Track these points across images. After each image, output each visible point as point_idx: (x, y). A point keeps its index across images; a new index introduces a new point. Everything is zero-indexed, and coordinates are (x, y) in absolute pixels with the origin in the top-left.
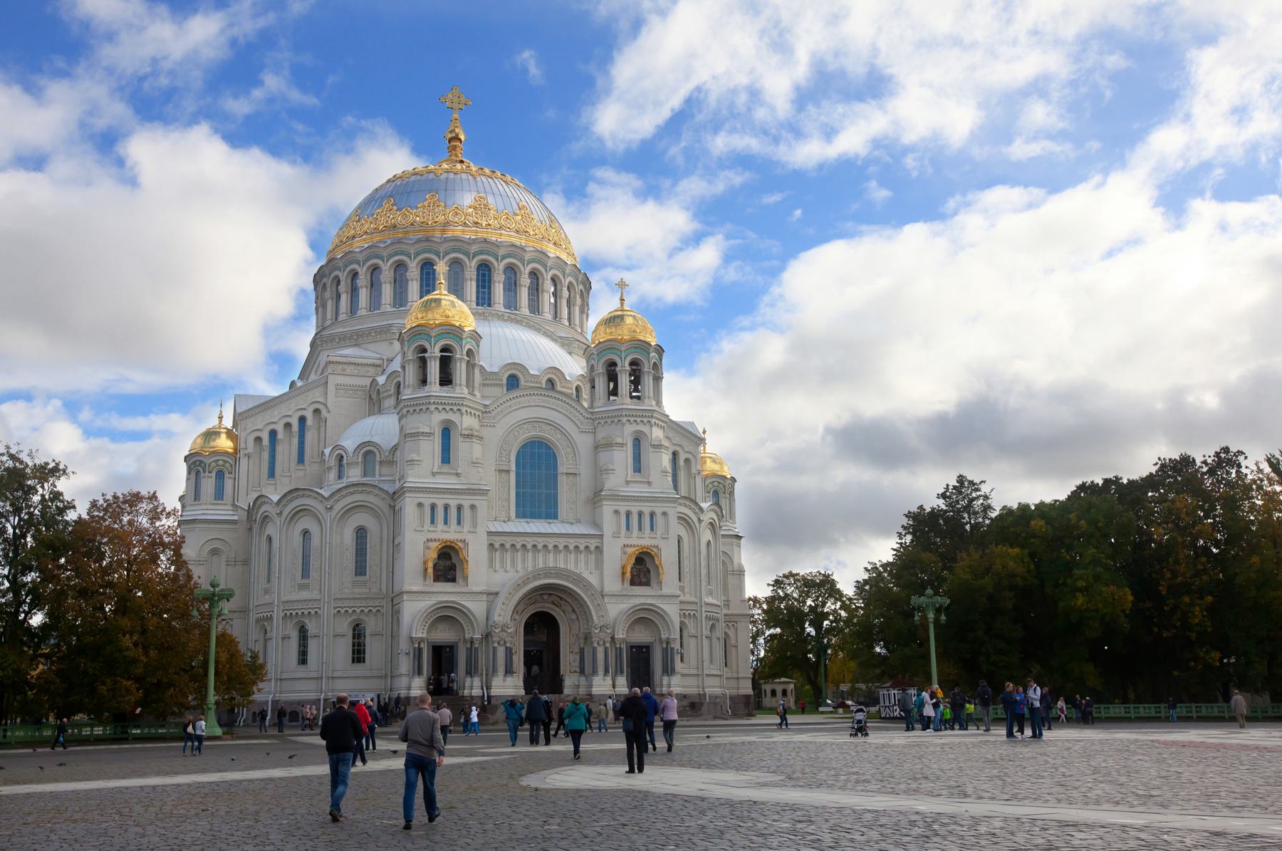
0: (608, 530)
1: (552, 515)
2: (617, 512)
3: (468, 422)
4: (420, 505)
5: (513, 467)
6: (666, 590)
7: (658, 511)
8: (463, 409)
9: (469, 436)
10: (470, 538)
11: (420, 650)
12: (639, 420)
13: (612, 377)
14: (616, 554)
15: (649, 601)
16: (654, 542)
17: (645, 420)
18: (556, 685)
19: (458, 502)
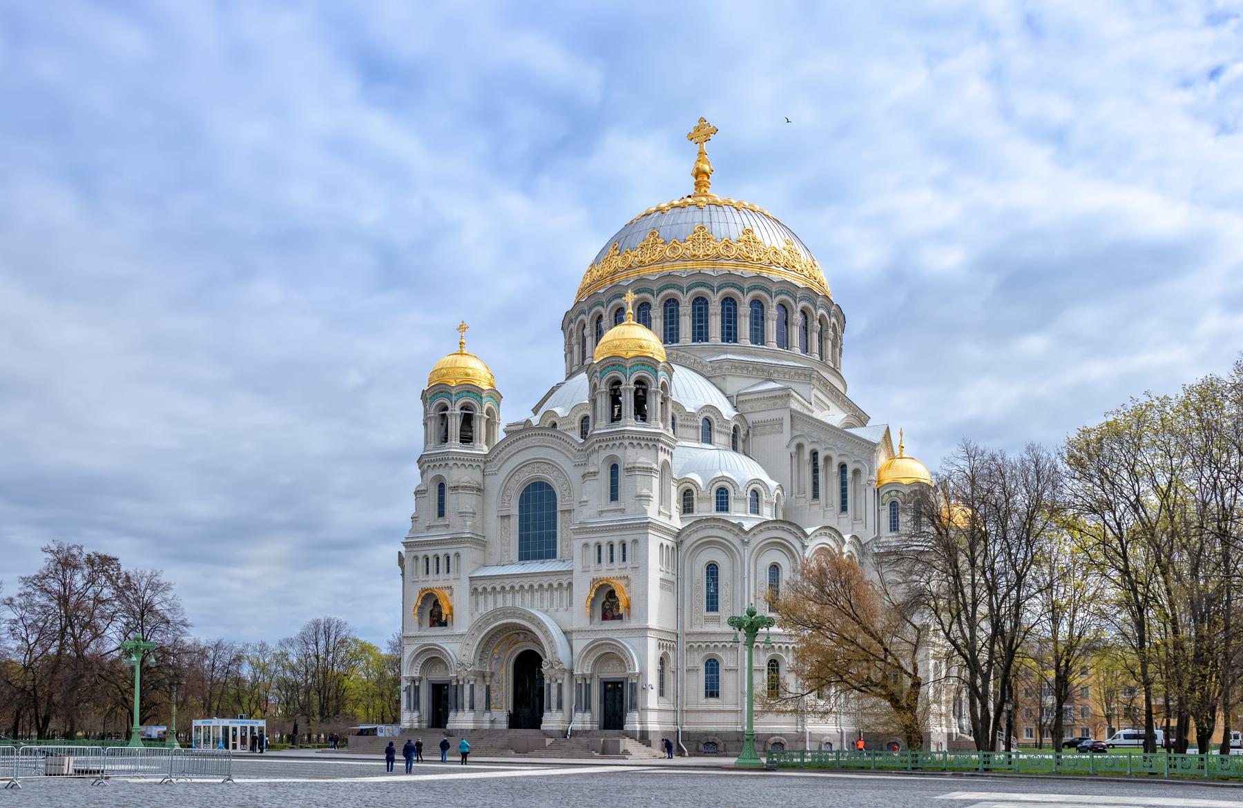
0: (577, 565)
1: (552, 555)
2: (586, 545)
3: (455, 476)
4: (416, 558)
5: (515, 511)
6: (633, 624)
7: (628, 540)
8: (451, 463)
9: (455, 488)
10: (454, 584)
11: (417, 689)
12: (610, 444)
13: (615, 399)
14: (583, 591)
15: (610, 635)
16: (624, 573)
17: (618, 443)
18: (536, 723)
19: (444, 552)
